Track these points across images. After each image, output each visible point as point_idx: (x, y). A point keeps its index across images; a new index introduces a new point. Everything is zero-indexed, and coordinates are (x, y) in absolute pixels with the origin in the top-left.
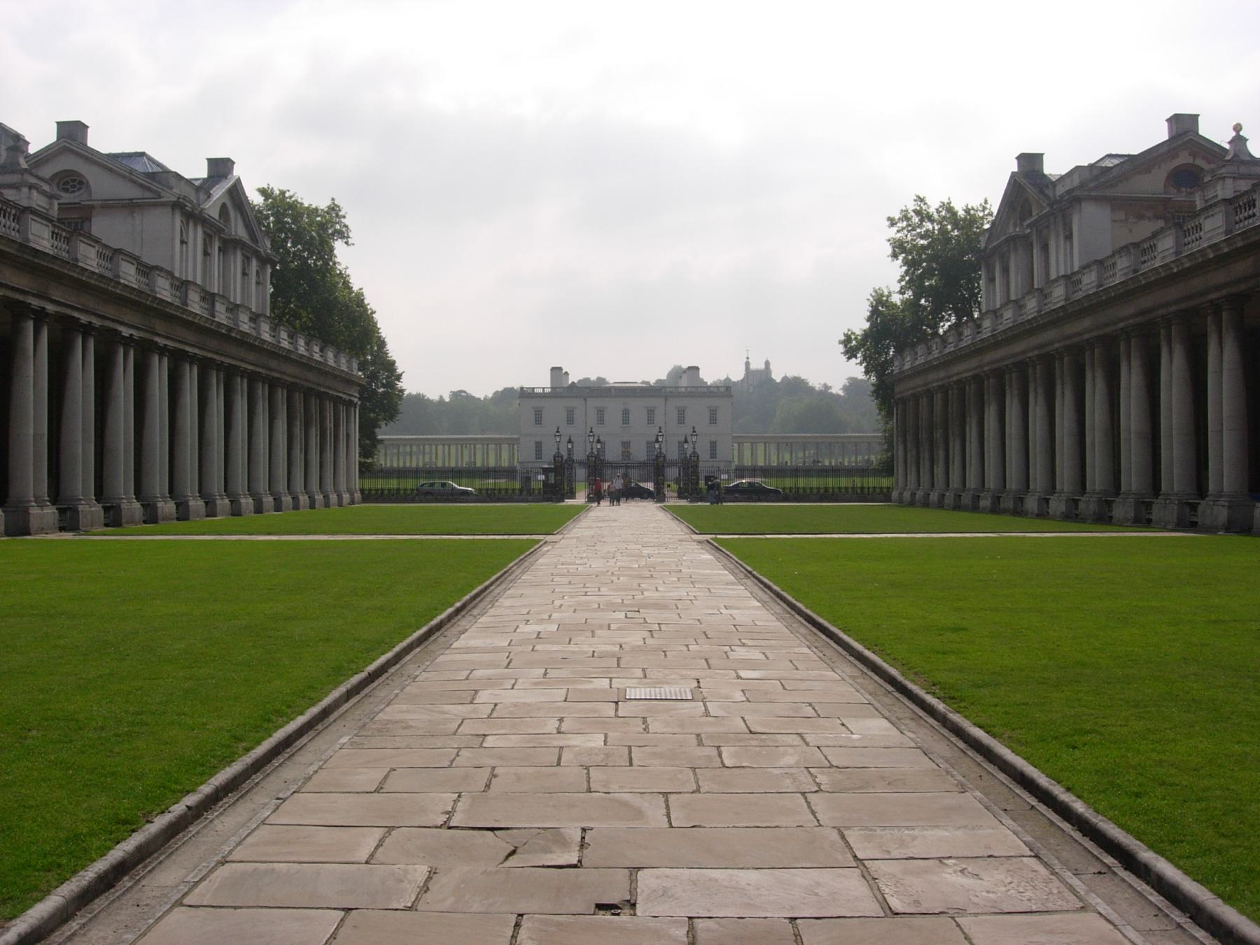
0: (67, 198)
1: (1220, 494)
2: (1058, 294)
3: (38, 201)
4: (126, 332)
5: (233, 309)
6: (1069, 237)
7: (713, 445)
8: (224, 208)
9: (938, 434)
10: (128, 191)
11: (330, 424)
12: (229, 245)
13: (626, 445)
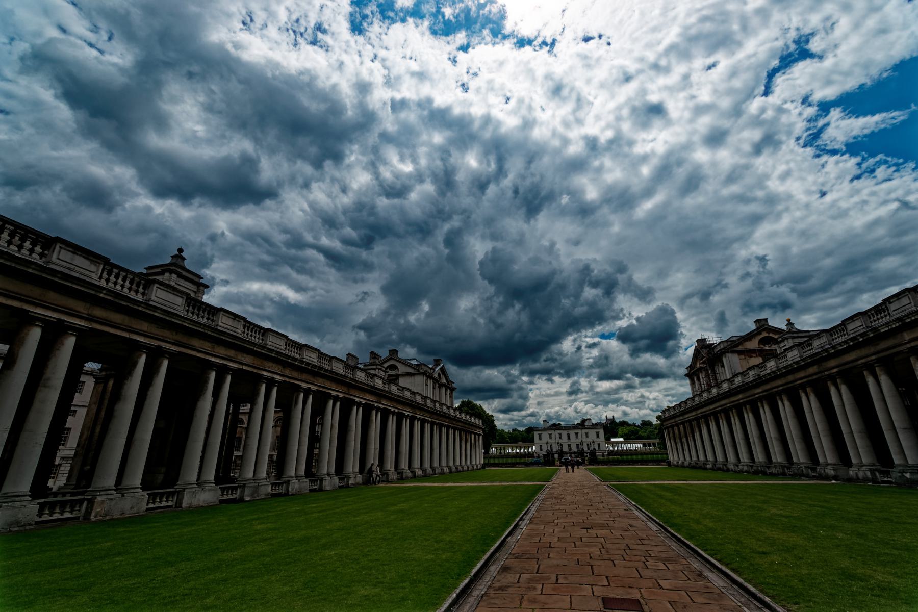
0: (391, 373)
1: (827, 464)
2: (725, 386)
3: (381, 373)
4: (406, 413)
5: (441, 405)
6: (723, 366)
7: (599, 445)
8: (439, 375)
9: (684, 440)
10: (410, 370)
11: (473, 442)
12: (441, 385)
13: (569, 445)
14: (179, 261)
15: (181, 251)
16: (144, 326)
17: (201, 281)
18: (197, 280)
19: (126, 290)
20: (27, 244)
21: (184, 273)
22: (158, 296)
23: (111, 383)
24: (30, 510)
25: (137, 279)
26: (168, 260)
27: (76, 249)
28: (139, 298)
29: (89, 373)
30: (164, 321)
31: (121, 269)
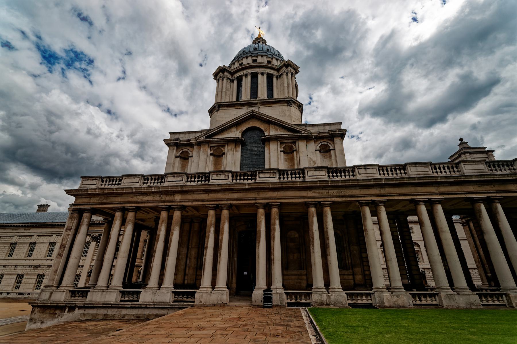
14: (465, 145)
15: (461, 140)
16: (471, 188)
17: (486, 149)
18: (483, 150)
19: (448, 173)
20: (398, 172)
21: (472, 150)
22: (467, 169)
23: (471, 225)
24: (474, 297)
25: (450, 166)
26: (458, 148)
27: (416, 164)
28: (457, 174)
29: (457, 222)
30: (481, 181)
31: (439, 164)
